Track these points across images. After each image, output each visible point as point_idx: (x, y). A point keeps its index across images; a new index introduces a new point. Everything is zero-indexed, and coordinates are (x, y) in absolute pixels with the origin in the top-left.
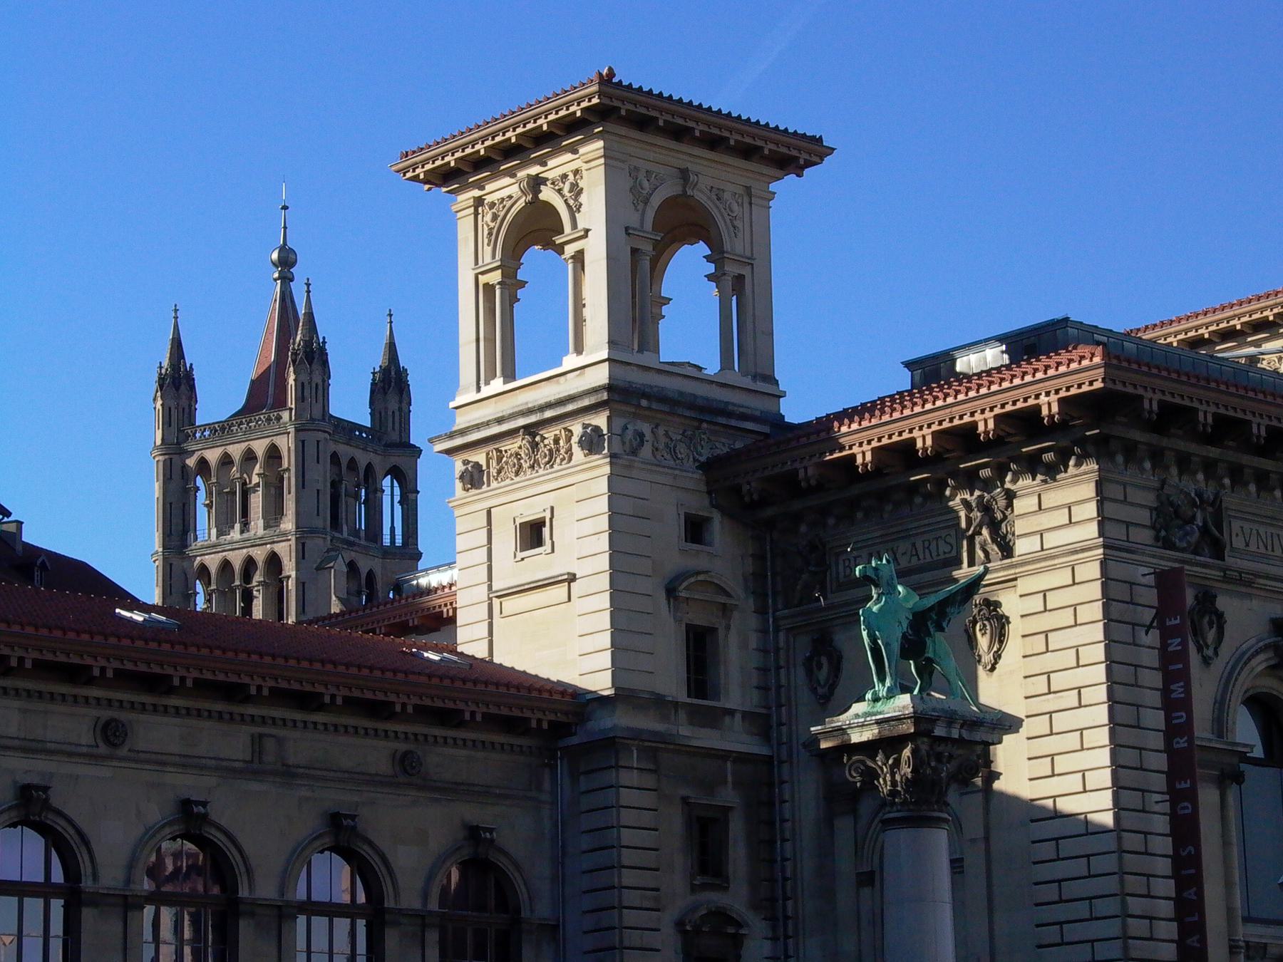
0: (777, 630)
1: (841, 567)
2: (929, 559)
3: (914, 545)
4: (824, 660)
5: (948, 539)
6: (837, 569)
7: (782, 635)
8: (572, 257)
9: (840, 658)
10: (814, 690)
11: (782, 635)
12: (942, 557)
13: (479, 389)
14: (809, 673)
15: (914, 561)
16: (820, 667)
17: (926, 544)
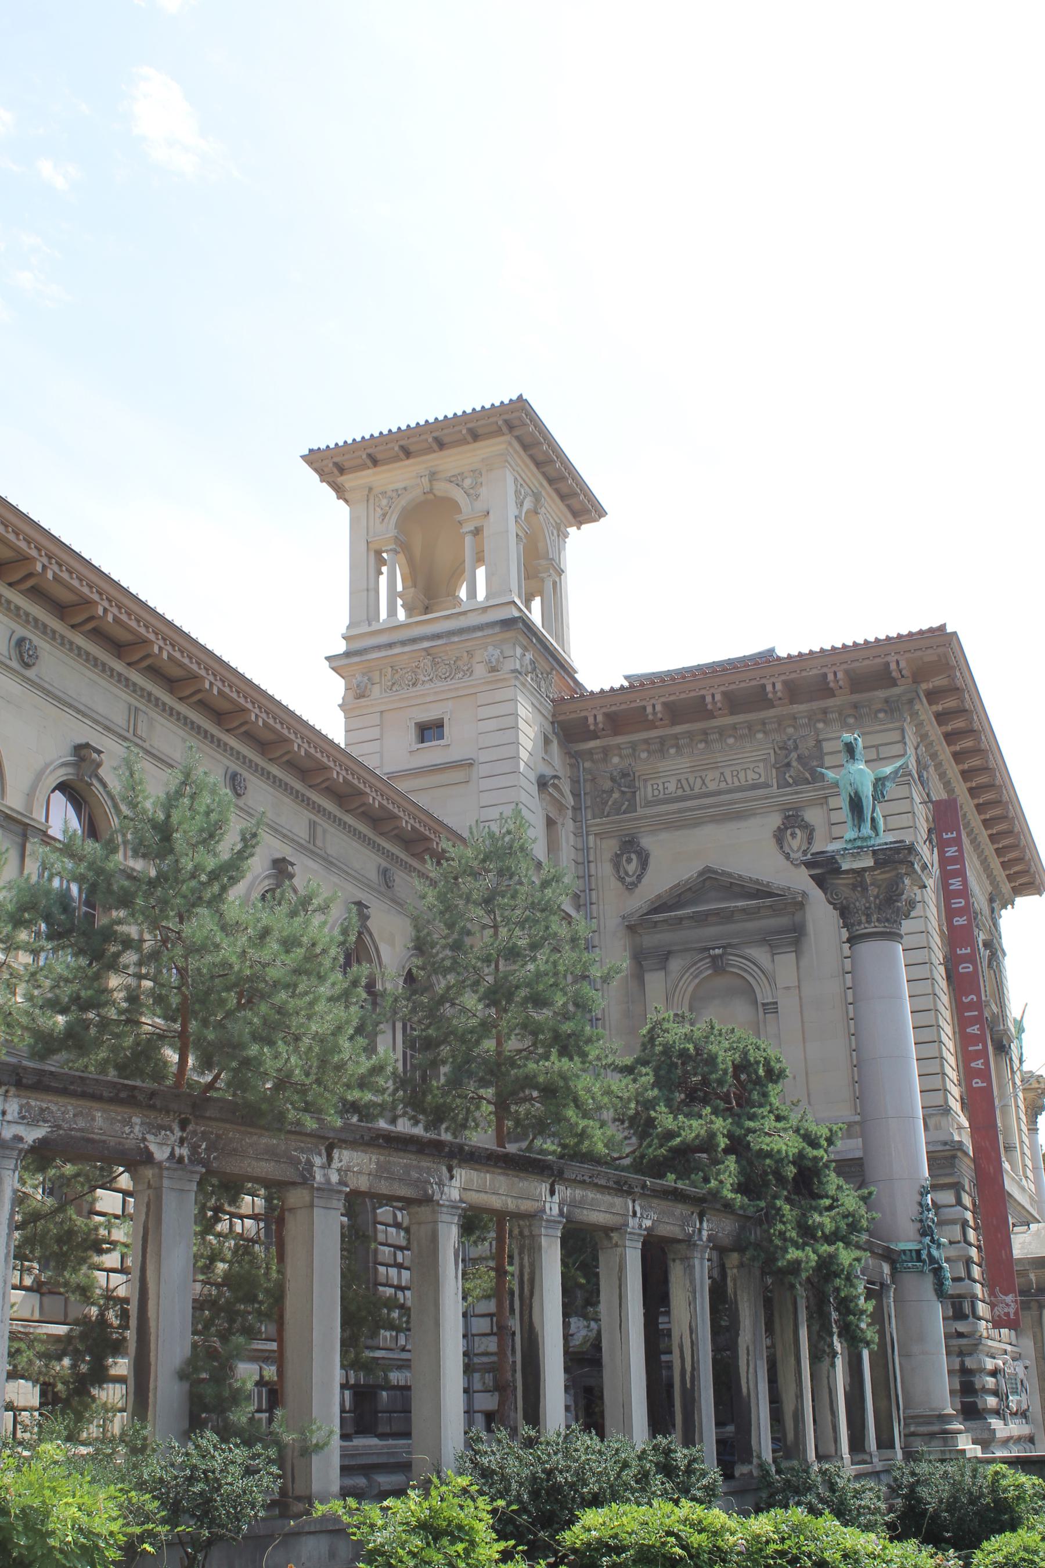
0: (587, 835)
1: (649, 789)
2: (737, 784)
3: (722, 773)
4: (634, 856)
5: (756, 770)
6: (645, 792)
7: (591, 838)
8: (471, 532)
9: (648, 856)
10: (621, 880)
11: (591, 838)
12: (751, 782)
13: (370, 625)
14: (617, 865)
15: (723, 785)
16: (629, 861)
17: (735, 773)
